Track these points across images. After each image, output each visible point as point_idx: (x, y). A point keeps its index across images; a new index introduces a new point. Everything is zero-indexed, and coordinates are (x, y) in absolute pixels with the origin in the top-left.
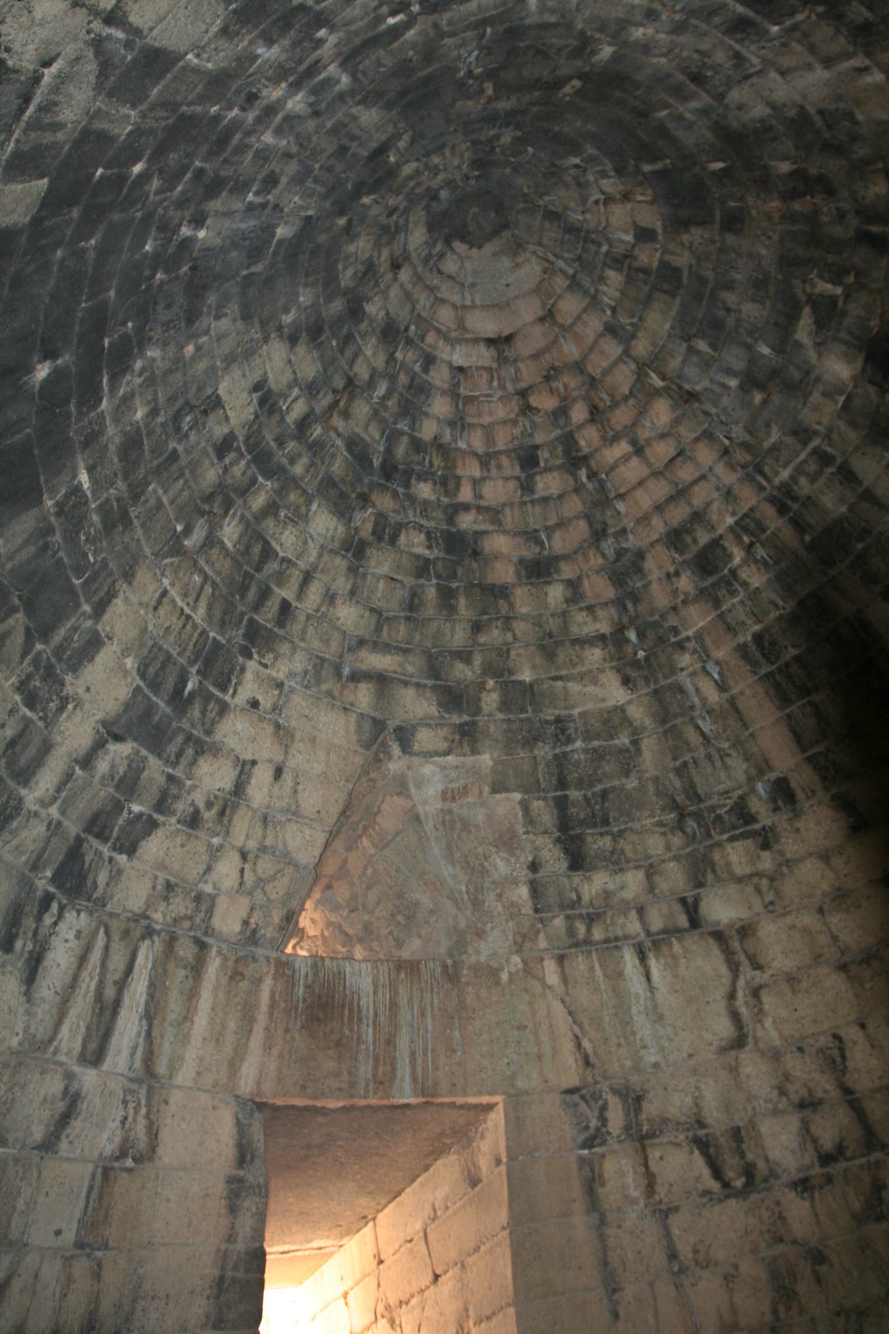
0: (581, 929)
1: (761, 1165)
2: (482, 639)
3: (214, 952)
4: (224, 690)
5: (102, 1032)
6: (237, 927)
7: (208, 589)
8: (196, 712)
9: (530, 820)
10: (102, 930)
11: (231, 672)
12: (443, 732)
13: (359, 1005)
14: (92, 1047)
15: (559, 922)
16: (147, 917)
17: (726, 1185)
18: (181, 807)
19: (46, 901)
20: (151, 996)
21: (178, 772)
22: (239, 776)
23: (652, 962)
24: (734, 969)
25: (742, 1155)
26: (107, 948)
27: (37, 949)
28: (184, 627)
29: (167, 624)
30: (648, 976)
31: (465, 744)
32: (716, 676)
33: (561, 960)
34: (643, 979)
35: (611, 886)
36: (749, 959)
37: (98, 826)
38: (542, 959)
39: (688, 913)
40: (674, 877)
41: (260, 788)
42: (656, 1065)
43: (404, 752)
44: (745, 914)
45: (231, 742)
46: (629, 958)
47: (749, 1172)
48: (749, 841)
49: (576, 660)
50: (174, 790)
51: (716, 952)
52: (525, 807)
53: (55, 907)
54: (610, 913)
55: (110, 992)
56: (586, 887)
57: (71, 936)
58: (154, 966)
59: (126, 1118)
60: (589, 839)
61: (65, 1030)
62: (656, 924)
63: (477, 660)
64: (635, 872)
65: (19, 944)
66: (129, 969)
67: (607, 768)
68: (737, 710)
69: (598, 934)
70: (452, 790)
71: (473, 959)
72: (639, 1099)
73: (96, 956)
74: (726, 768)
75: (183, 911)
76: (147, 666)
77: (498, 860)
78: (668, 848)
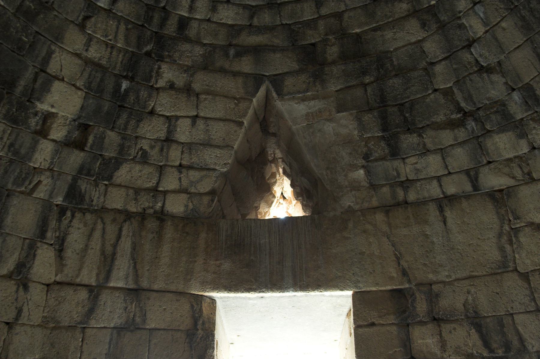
0: (401, 194)
1: (516, 343)
2: (324, 11)
3: (169, 223)
4: (149, 81)
5: (107, 268)
6: (182, 209)
7: (122, 27)
8: (132, 98)
9: (362, 127)
10: (99, 221)
11: (151, 71)
12: (303, 77)
13: (260, 244)
14: (102, 276)
15: (386, 190)
16: (126, 211)
17: (491, 351)
18: (133, 152)
19: (62, 211)
20: (134, 249)
21: (129, 132)
22: (169, 127)
23: (448, 213)
24: (502, 220)
25: (504, 334)
26: (104, 229)
27: (62, 234)
28: (111, 53)
29: (99, 55)
30: (445, 222)
31: (317, 84)
32: (482, 15)
33: (387, 213)
34: (442, 224)
35: (418, 166)
36: (512, 212)
37: (83, 170)
38: (375, 213)
39: (472, 181)
40: (461, 158)
41: (184, 132)
42: (447, 276)
43: (278, 95)
44: (511, 182)
45: (158, 109)
46: (432, 210)
47: (507, 347)
48: (510, 133)
49: (389, 14)
50: (127, 144)
51: (490, 206)
52: (359, 119)
53: (69, 214)
54: (419, 184)
55: (109, 249)
56: (402, 165)
57: (81, 226)
58: (133, 235)
59: (127, 308)
60: (402, 137)
61: (85, 272)
62: (451, 190)
63: (321, 25)
64: (434, 156)
65: (49, 234)
66: (119, 237)
67: (412, 88)
68: (496, 39)
69: (412, 197)
70: (312, 113)
71: (332, 214)
72: (437, 296)
73: (97, 234)
74: (492, 83)
75: (147, 205)
76: (90, 83)
77: (344, 154)
78: (456, 139)
